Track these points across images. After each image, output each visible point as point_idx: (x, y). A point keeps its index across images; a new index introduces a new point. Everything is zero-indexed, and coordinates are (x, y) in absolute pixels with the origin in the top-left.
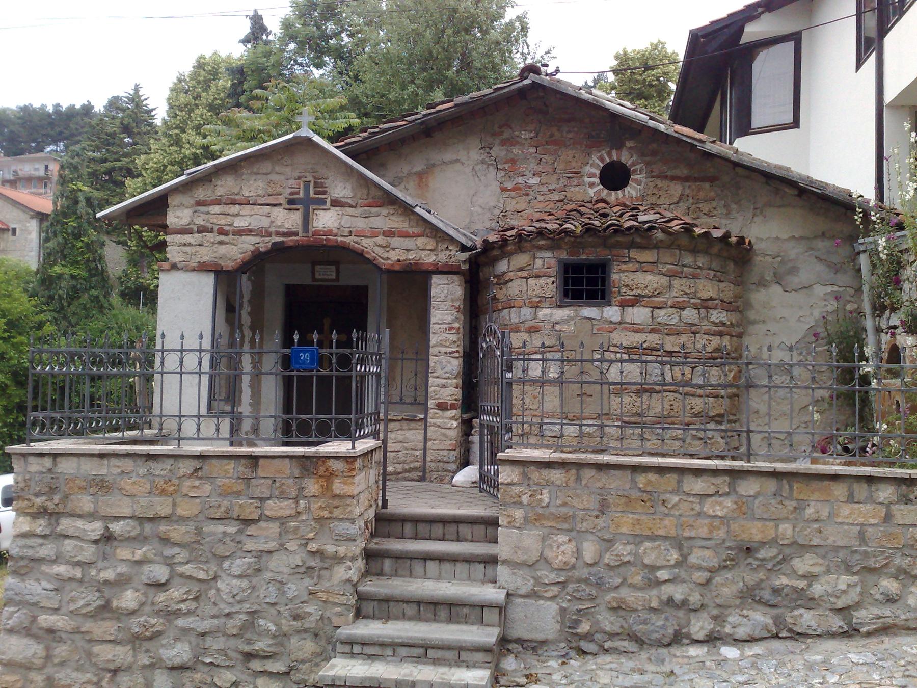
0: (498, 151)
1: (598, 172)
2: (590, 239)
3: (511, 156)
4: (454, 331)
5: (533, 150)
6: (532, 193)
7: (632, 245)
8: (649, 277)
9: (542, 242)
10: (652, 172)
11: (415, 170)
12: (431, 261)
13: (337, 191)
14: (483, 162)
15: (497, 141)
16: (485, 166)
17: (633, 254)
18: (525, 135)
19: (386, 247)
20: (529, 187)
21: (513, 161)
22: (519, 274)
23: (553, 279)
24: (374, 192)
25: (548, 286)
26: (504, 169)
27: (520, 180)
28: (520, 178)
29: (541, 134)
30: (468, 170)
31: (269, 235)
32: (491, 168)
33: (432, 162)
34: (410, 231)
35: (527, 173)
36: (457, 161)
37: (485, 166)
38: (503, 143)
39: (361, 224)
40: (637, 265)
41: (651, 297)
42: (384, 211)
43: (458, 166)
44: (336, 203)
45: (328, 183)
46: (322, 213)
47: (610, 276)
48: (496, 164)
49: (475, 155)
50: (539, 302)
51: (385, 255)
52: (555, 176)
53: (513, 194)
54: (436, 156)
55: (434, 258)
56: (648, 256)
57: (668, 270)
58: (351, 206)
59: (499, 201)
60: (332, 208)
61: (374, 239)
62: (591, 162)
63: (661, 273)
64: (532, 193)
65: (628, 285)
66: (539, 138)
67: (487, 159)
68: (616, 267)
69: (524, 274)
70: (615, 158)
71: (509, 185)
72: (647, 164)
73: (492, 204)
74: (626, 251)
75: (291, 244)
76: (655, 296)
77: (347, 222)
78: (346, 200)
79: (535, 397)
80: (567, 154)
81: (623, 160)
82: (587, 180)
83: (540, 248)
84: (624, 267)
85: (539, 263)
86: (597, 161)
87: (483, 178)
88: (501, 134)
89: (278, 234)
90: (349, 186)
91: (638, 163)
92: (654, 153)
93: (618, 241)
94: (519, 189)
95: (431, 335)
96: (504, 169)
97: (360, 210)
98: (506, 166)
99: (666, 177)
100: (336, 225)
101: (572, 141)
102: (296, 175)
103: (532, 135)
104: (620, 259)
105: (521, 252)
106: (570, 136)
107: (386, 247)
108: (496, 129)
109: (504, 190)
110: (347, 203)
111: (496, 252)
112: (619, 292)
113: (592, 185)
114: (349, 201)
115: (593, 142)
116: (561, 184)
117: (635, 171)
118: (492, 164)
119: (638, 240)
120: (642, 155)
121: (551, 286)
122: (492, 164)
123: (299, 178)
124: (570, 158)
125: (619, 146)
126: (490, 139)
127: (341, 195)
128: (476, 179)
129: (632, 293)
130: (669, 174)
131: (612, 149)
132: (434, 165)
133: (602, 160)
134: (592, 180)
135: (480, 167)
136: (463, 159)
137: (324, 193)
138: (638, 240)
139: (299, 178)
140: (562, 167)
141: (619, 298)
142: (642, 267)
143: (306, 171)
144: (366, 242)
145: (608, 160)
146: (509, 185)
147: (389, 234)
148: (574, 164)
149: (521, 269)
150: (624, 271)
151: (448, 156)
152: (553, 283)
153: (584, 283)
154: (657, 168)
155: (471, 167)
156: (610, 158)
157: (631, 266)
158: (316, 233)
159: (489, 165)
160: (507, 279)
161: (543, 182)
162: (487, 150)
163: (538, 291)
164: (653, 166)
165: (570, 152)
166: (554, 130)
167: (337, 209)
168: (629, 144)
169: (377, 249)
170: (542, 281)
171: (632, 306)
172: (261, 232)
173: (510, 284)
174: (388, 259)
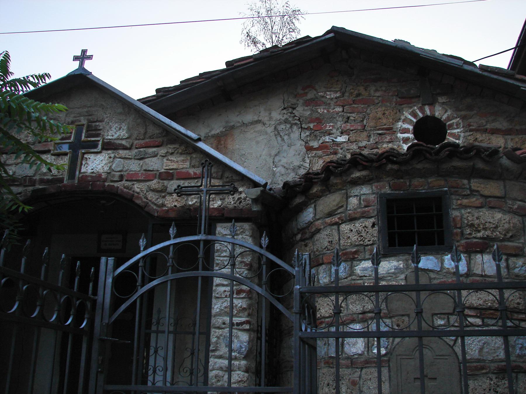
0: (301, 111)
1: (411, 128)
2: (419, 166)
3: (315, 115)
4: (243, 295)
5: (340, 109)
6: (340, 151)
7: (473, 173)
8: (499, 216)
9: (357, 174)
10: (469, 125)
11: (213, 132)
12: (216, 206)
13: (110, 133)
14: (286, 121)
15: (301, 101)
16: (288, 126)
17: (475, 184)
18: (331, 95)
19: (161, 191)
20: (338, 144)
21: (319, 121)
22: (328, 220)
23: (372, 220)
24: (152, 130)
25: (365, 231)
26: (308, 129)
27: (327, 139)
28: (327, 137)
29: (347, 94)
30: (270, 130)
31: (32, 182)
32: (295, 128)
33: (232, 124)
34: (191, 171)
35: (334, 131)
36: (258, 122)
37: (288, 126)
38: (307, 103)
39: (134, 166)
40: (481, 200)
41: (503, 240)
42: (162, 151)
43: (259, 127)
44: (109, 146)
45: (101, 125)
46: (92, 156)
47: (448, 213)
48: (300, 123)
49: (276, 115)
50: (356, 252)
51: (160, 201)
52: (365, 134)
53: (320, 153)
54: (234, 118)
55: (219, 203)
56: (492, 188)
57: (519, 207)
58: (125, 148)
59: (304, 160)
60: (104, 152)
61: (148, 183)
62: (403, 118)
63: (511, 211)
64: (340, 151)
65: (472, 225)
66: (346, 98)
67: (290, 119)
68: (455, 202)
69: (335, 219)
70: (428, 112)
71: (315, 144)
72: (464, 118)
73: (297, 163)
74: (465, 182)
75: (52, 190)
76: (509, 240)
77: (118, 164)
78: (120, 142)
79: (354, 383)
80: (375, 112)
81: (437, 114)
82: (400, 136)
83: (356, 183)
84: (465, 201)
85: (354, 201)
86: (410, 117)
87: (286, 138)
88: (306, 94)
89: (42, 181)
90: (124, 127)
91: (454, 118)
92: (470, 108)
93: (455, 168)
94: (326, 147)
95: (214, 301)
96: (308, 129)
97: (134, 152)
98: (312, 125)
99: (485, 131)
100: (106, 169)
101: (380, 99)
102: (70, 119)
103: (338, 95)
104: (460, 190)
105: (330, 192)
106: (378, 94)
107: (161, 191)
108: (301, 92)
109: (309, 149)
110: (121, 145)
111: (299, 200)
112: (462, 233)
113: (406, 140)
114: (124, 142)
115: (406, 100)
116: (372, 141)
117: (451, 126)
118: (296, 124)
119: (480, 165)
120: (457, 109)
121: (370, 230)
122: (296, 124)
123: (72, 123)
124: (380, 115)
125: (432, 104)
126: (293, 101)
127: (116, 136)
128: (279, 138)
129: (479, 235)
130: (488, 126)
131: (424, 105)
132: (233, 128)
133: (415, 115)
134: (406, 135)
135: (283, 126)
136: (265, 119)
137: (98, 135)
138: (480, 165)
139: (72, 123)
140: (372, 124)
141: (463, 242)
142: (489, 203)
143: (80, 115)
144: (137, 187)
145: (421, 115)
146: (315, 144)
147: (168, 175)
148: (384, 121)
149: (331, 214)
150: (466, 207)
151: (249, 117)
152: (373, 226)
153: (413, 225)
154: (475, 122)
155: (273, 127)
156: (423, 113)
157: (475, 200)
158: (84, 178)
159: (292, 125)
160: (313, 229)
161: (353, 139)
162: (290, 110)
163: (354, 238)
164: (470, 120)
165: (379, 109)
166: (362, 89)
167: (110, 152)
168: (441, 100)
169: (151, 196)
170: (358, 225)
171: (482, 252)
172: (25, 180)
173: (317, 236)
174: (163, 205)
